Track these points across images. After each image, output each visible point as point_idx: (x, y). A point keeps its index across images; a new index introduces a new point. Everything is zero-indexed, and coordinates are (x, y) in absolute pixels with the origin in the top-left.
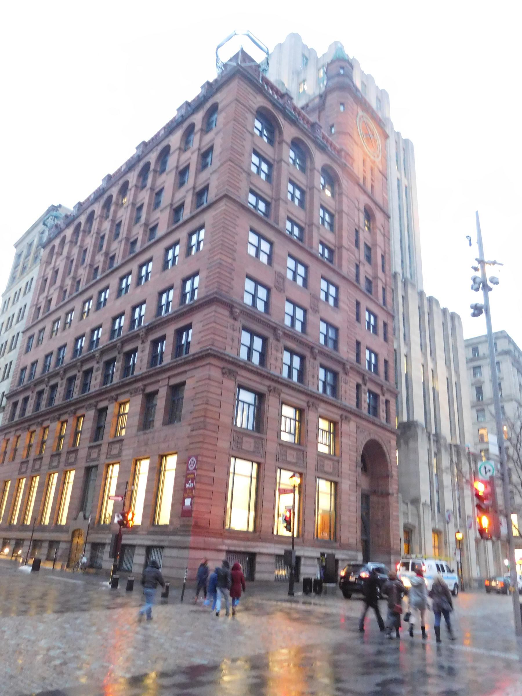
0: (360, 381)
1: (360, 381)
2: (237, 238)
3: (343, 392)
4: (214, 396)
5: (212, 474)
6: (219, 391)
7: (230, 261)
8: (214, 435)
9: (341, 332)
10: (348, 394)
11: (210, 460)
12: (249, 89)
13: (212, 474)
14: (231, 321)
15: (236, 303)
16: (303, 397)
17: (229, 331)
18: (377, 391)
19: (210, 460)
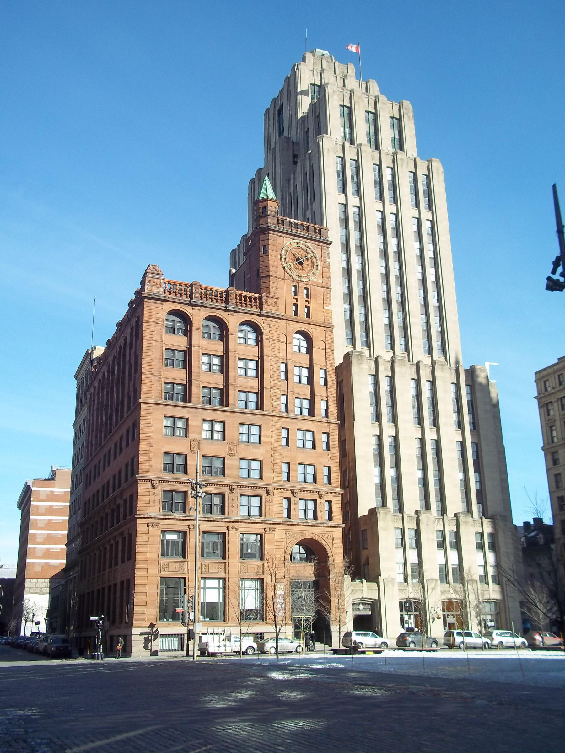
0: (289, 495)
1: (289, 495)
2: (152, 429)
3: (267, 509)
4: (144, 543)
5: (145, 591)
6: (146, 539)
7: (147, 448)
8: (145, 567)
9: (263, 462)
10: (272, 509)
11: (143, 583)
12: (155, 305)
13: (145, 591)
14: (153, 490)
15: (153, 478)
16: (223, 524)
17: (152, 497)
18: (316, 497)
19: (143, 583)
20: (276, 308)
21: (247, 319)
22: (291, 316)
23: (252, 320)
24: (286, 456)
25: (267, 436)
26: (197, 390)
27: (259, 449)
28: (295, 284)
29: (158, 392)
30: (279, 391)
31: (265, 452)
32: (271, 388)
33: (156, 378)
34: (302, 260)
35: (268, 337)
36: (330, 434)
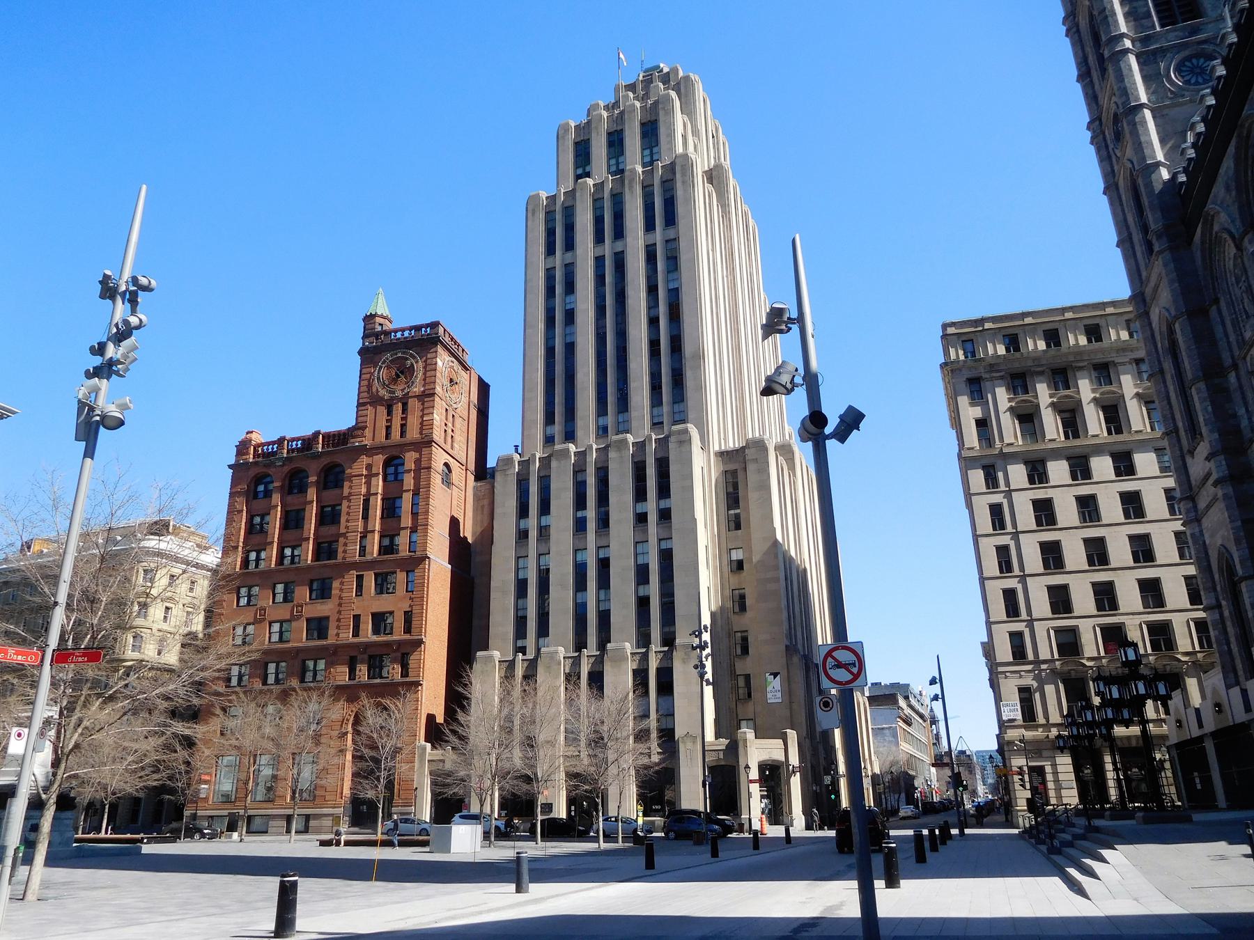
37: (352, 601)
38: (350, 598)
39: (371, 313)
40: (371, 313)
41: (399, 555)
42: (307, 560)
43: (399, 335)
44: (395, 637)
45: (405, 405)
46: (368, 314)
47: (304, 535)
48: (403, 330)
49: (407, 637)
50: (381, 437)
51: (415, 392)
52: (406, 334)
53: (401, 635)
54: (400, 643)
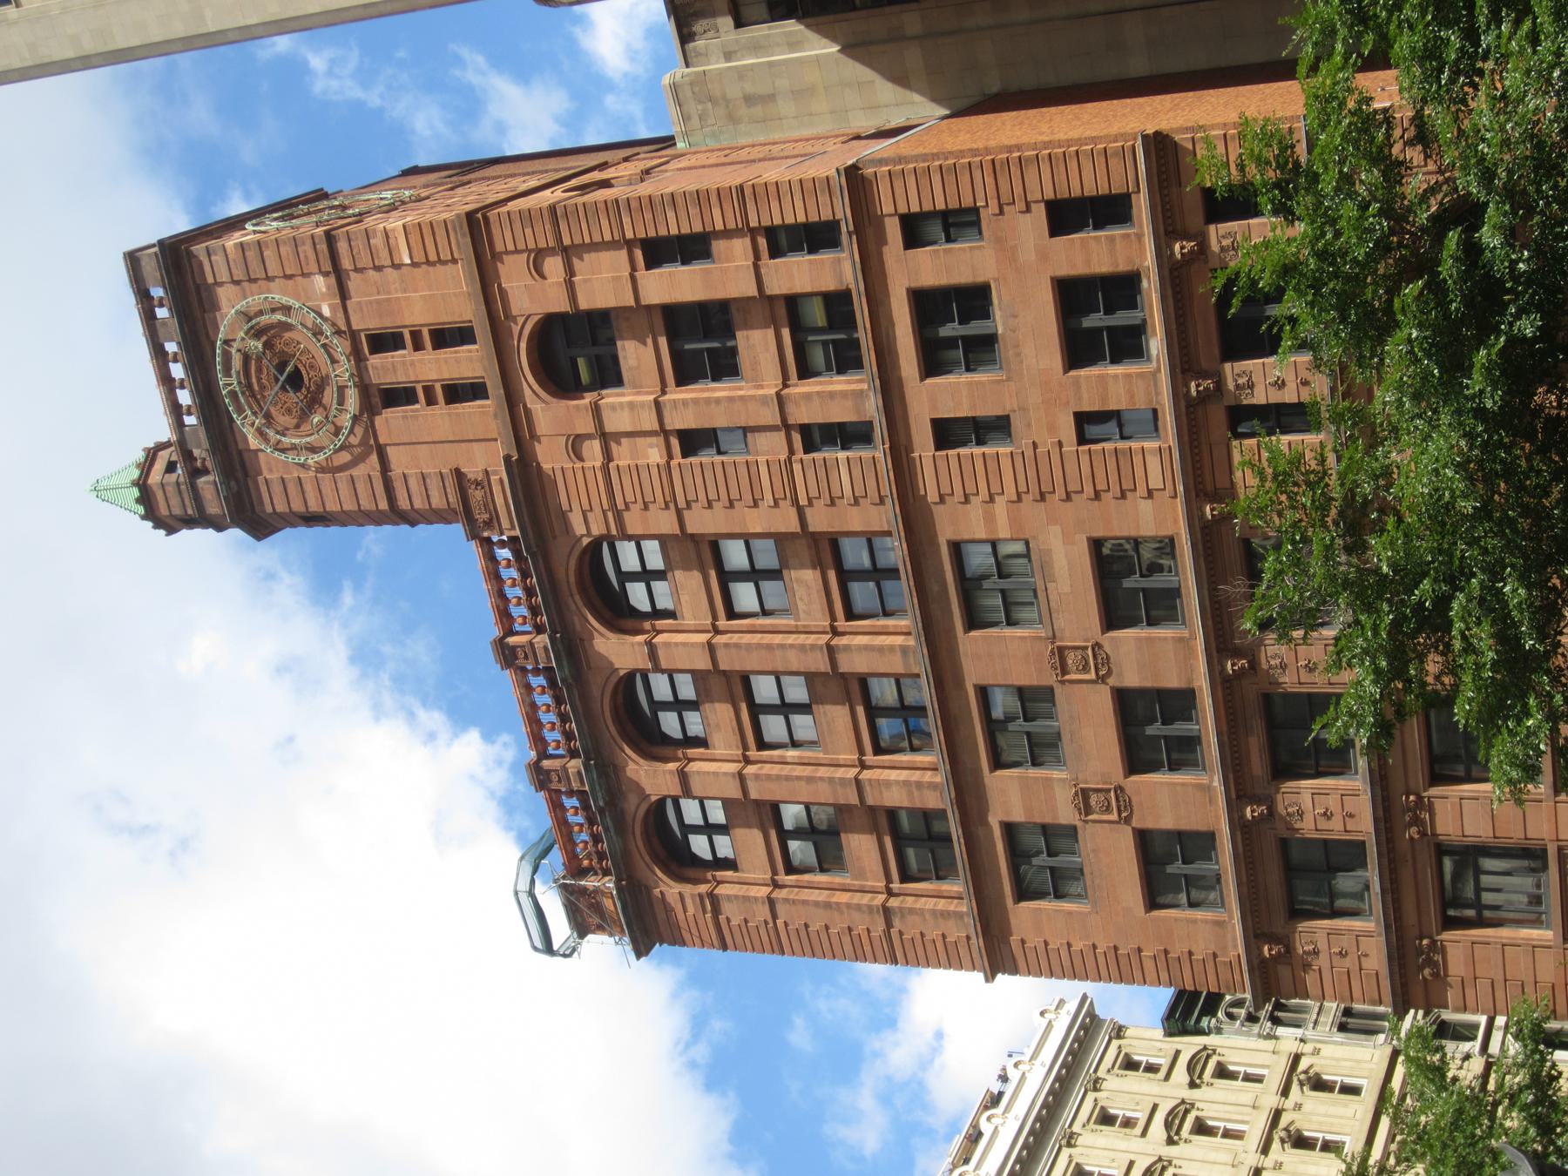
20: (493, 478)
21: (577, 598)
22: (496, 416)
23: (572, 579)
24: (1052, 428)
25: (990, 519)
26: (894, 788)
27: (1049, 551)
28: (377, 400)
29: (940, 920)
30: (797, 467)
31: (1055, 530)
32: (795, 502)
33: (897, 922)
34: (282, 379)
35: (610, 514)
36: (903, 209)
37: (1029, 453)
38: (1018, 460)
39: (138, 501)
40: (138, 501)
41: (852, 286)
42: (904, 650)
43: (184, 397)
44: (1149, 261)
45: (385, 342)
46: (141, 510)
47: (823, 669)
48: (166, 381)
49: (1142, 205)
50: (484, 415)
51: (332, 308)
52: (177, 371)
53: (1140, 237)
54: (1168, 228)
